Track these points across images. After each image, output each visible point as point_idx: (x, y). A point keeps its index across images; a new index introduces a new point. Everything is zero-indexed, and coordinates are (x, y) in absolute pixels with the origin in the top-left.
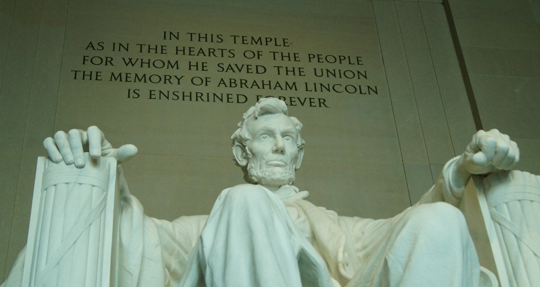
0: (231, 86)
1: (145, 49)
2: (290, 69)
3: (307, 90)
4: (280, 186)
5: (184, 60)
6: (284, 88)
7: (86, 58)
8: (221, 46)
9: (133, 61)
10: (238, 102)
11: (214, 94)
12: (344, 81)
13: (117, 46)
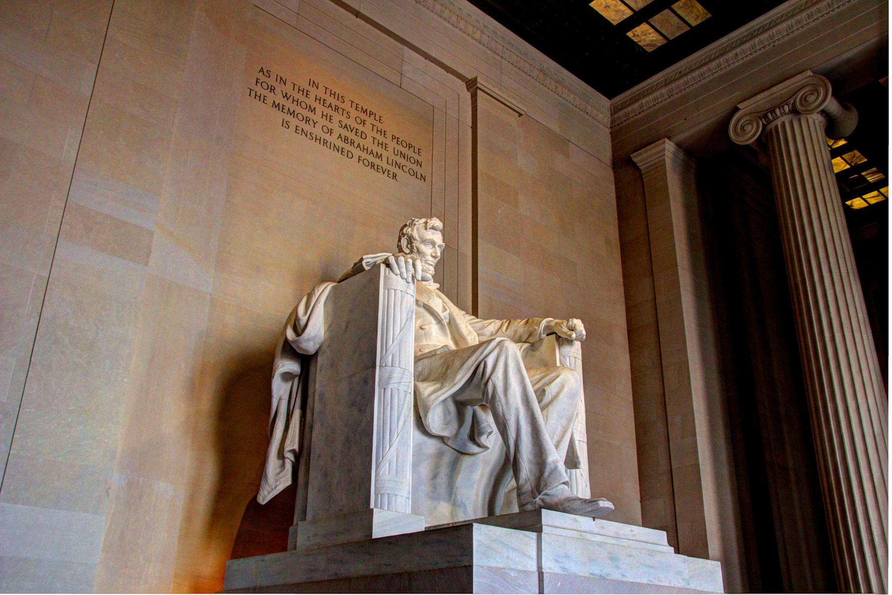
1: (297, 88)
5: (320, 108)
12: (408, 164)
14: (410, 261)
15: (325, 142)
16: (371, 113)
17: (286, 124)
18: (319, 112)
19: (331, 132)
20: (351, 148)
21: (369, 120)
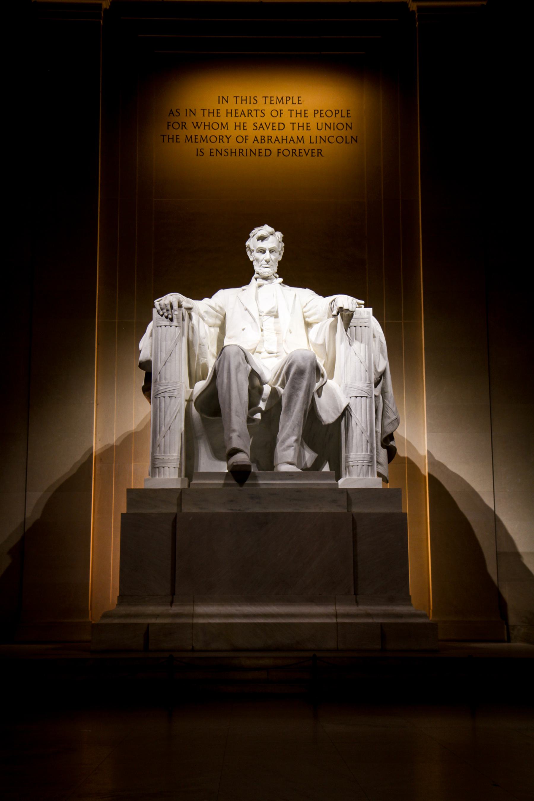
0: (261, 143)
1: (206, 112)
2: (301, 125)
3: (311, 143)
5: (231, 121)
6: (296, 142)
7: (169, 124)
8: (256, 107)
9: (199, 125)
10: (265, 156)
13: (188, 111)
15: (241, 152)
18: (231, 126)
19: (246, 139)
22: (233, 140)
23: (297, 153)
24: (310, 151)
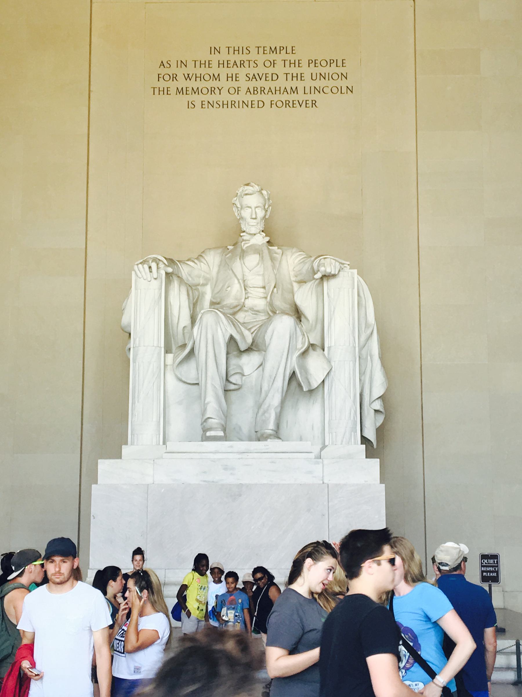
2: (295, 75)
4: (255, 234)
5: (224, 72)
6: (289, 92)
8: (249, 57)
9: (190, 76)
11: (243, 102)
12: (331, 83)
14: (146, 266)
16: (282, 48)
17: (191, 105)
18: (223, 77)
20: (263, 97)
21: (278, 58)
22: (224, 92)
23: (291, 104)
24: (304, 102)
